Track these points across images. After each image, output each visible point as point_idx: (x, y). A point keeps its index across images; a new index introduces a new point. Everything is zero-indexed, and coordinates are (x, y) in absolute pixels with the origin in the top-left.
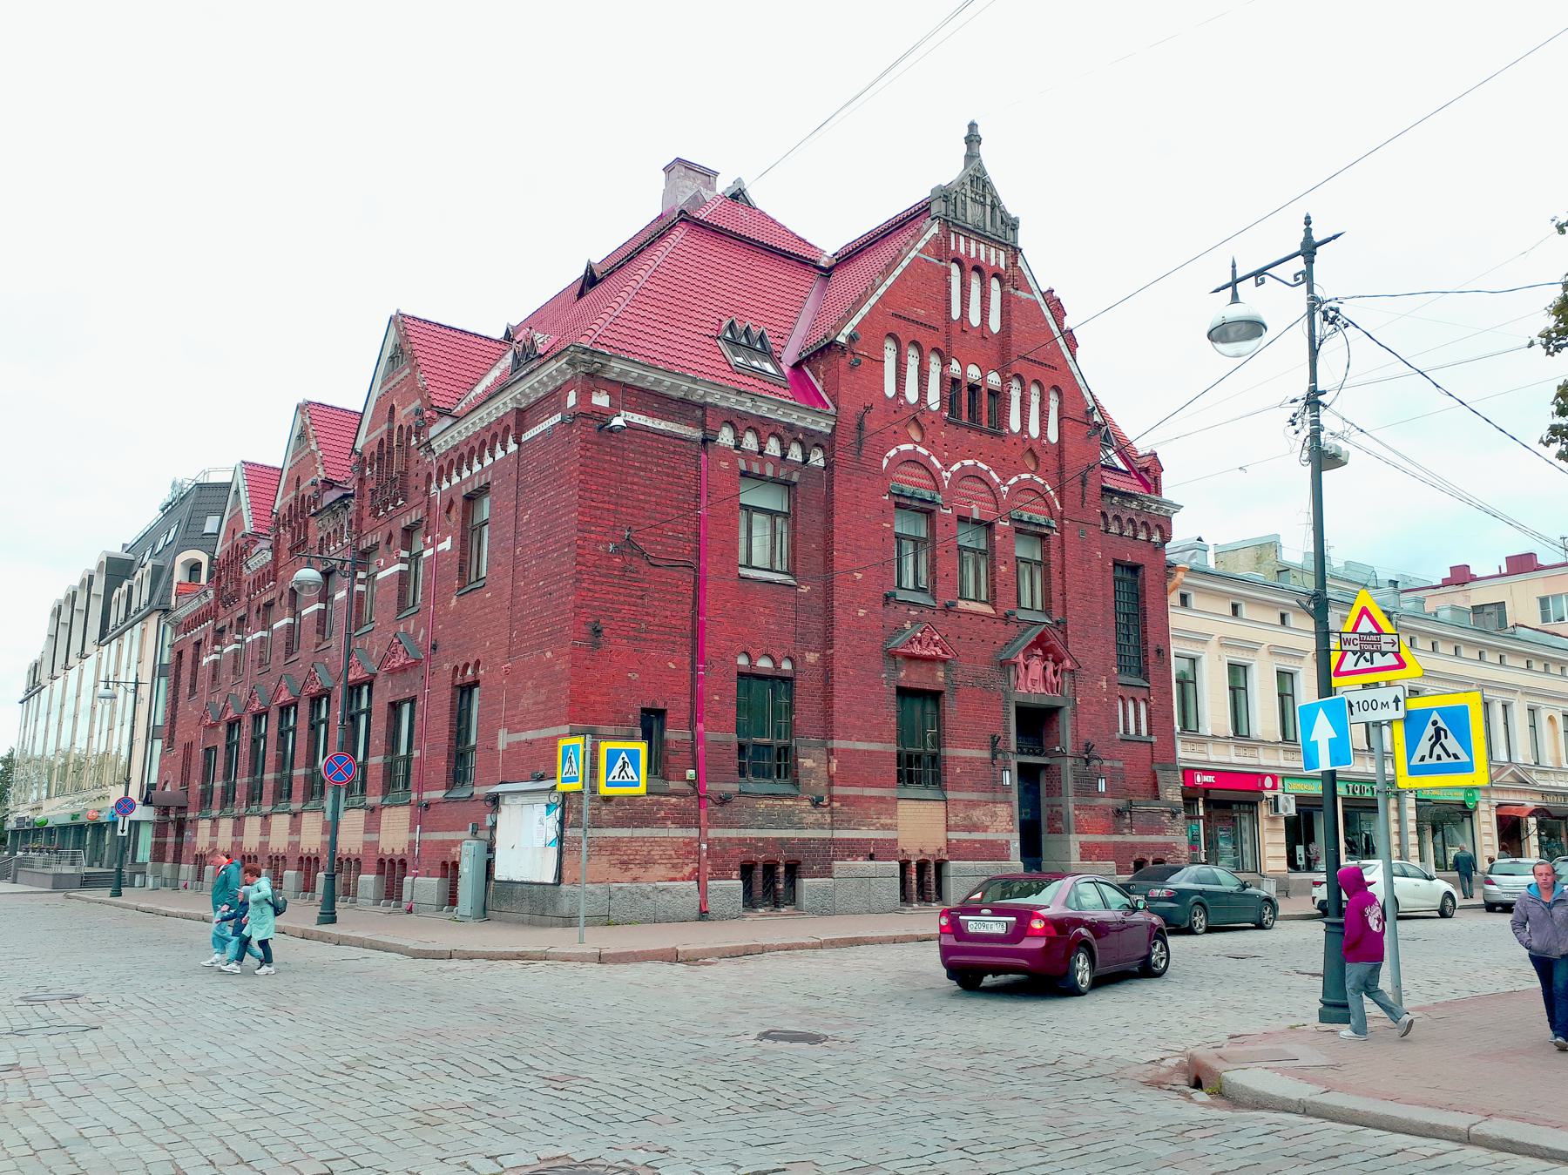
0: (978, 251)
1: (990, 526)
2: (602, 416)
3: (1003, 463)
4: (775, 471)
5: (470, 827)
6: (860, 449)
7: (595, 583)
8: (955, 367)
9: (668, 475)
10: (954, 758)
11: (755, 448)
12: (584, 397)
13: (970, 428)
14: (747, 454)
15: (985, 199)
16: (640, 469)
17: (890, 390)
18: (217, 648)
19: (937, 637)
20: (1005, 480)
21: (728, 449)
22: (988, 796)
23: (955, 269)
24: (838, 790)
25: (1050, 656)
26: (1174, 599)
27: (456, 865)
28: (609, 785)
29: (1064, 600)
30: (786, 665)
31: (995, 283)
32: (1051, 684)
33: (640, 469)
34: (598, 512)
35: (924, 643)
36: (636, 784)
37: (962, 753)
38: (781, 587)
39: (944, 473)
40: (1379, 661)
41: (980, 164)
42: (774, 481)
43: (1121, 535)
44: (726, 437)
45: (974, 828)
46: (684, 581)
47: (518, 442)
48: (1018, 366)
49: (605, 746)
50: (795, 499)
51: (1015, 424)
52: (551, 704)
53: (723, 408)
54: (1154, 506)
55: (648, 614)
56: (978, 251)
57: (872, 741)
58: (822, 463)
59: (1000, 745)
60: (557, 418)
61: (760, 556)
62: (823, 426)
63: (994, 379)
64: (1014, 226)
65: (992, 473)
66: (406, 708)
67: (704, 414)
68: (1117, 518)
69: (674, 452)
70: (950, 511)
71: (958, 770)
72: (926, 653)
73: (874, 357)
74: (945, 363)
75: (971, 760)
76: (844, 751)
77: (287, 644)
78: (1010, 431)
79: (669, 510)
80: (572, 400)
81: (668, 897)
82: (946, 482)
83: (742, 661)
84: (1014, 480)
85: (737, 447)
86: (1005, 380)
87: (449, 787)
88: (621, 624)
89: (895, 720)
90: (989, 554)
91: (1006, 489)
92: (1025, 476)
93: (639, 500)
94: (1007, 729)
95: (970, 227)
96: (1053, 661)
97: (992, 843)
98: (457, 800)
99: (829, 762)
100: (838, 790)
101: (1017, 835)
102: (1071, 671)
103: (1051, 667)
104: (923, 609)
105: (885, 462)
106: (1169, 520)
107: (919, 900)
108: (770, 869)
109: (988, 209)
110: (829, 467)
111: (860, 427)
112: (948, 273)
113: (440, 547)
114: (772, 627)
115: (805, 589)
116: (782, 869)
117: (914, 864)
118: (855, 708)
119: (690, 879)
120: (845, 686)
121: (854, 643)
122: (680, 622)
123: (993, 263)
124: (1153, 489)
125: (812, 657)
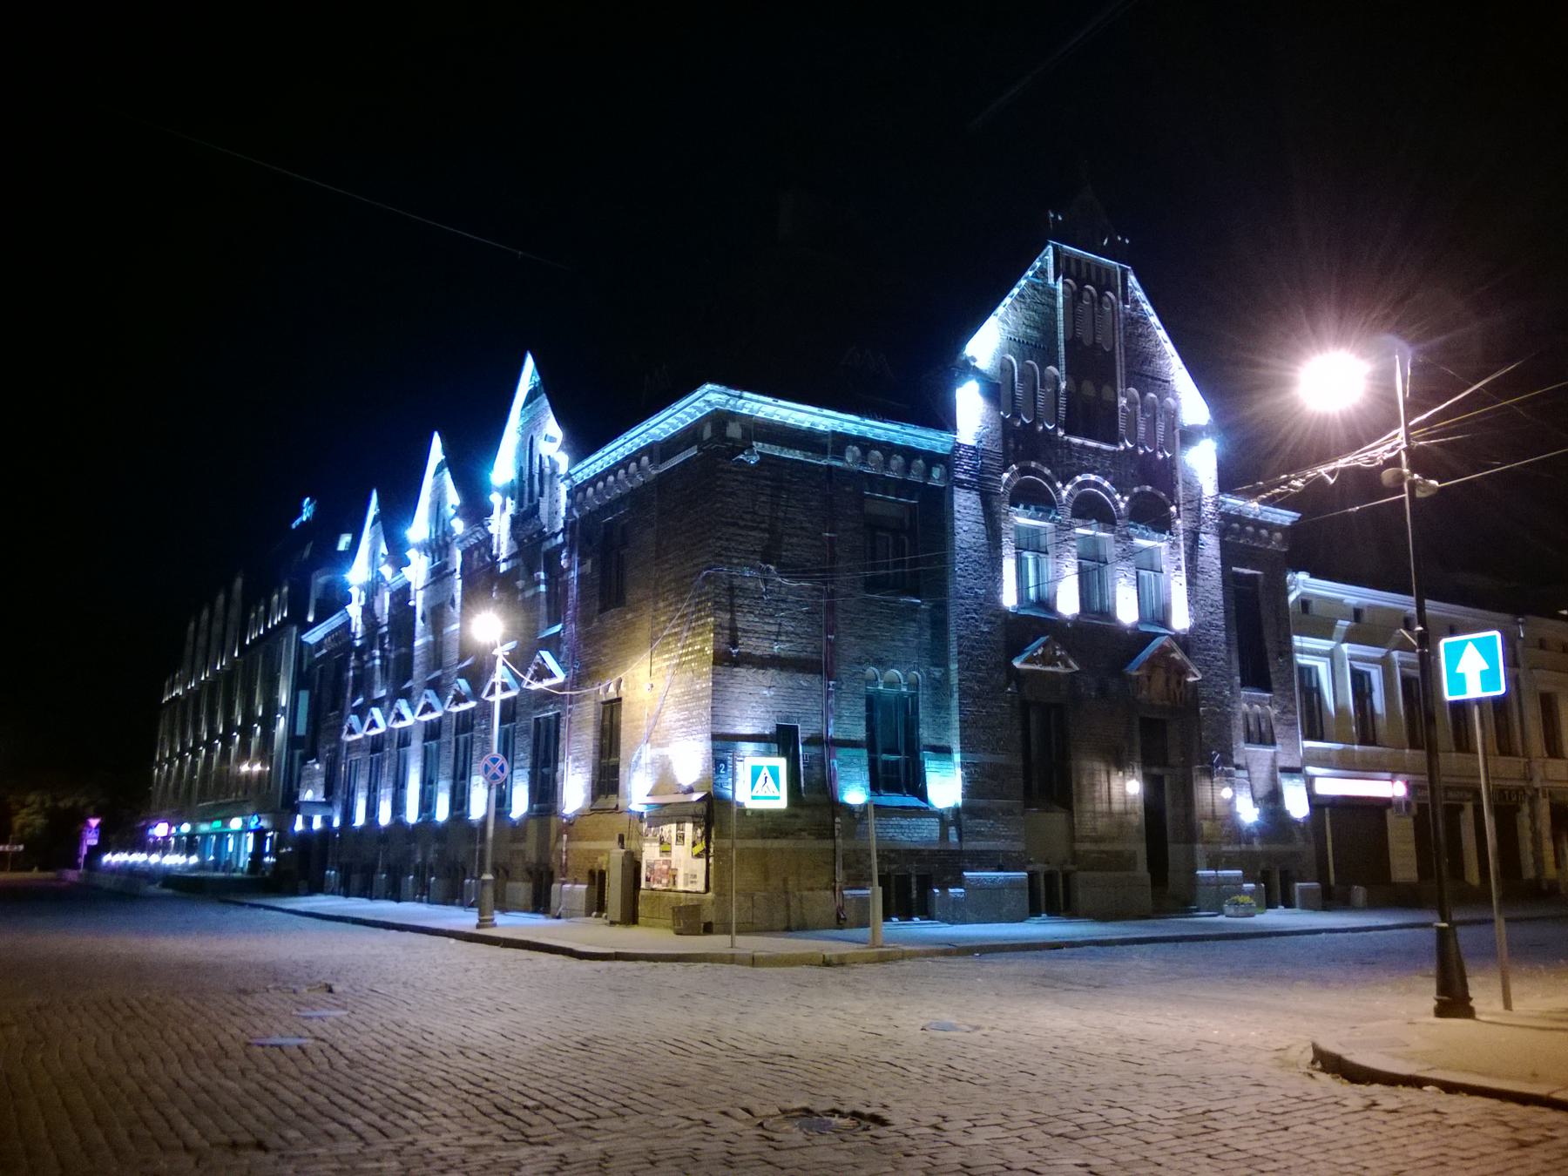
27: (602, 874)
36: (778, 798)
97: (1119, 854)
108: (904, 881)
116: (914, 880)
119: (826, 889)
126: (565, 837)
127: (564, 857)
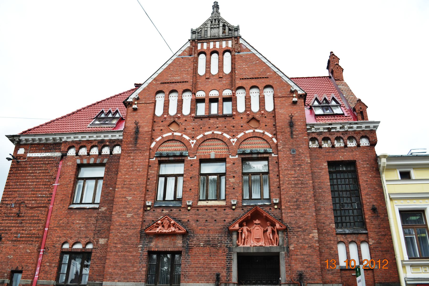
2: (23, 156)
3: (233, 128)
9: (43, 173)
14: (81, 157)
15: (219, 25)
19: (173, 222)
33: (31, 173)
34: (11, 193)
35: (166, 226)
38: (90, 210)
46: (42, 214)
53: (69, 142)
55: (23, 230)
57: (128, 281)
64: (237, 29)
70: (195, 158)
73: (148, 102)
79: (41, 186)
82: (192, 145)
88: (10, 235)
89: (144, 269)
91: (235, 140)
93: (29, 185)
103: (270, 229)
104: (172, 209)
109: (221, 28)
114: (82, 229)
115: (103, 209)
118: (119, 264)
120: (113, 253)
121: (122, 231)
122: (37, 232)
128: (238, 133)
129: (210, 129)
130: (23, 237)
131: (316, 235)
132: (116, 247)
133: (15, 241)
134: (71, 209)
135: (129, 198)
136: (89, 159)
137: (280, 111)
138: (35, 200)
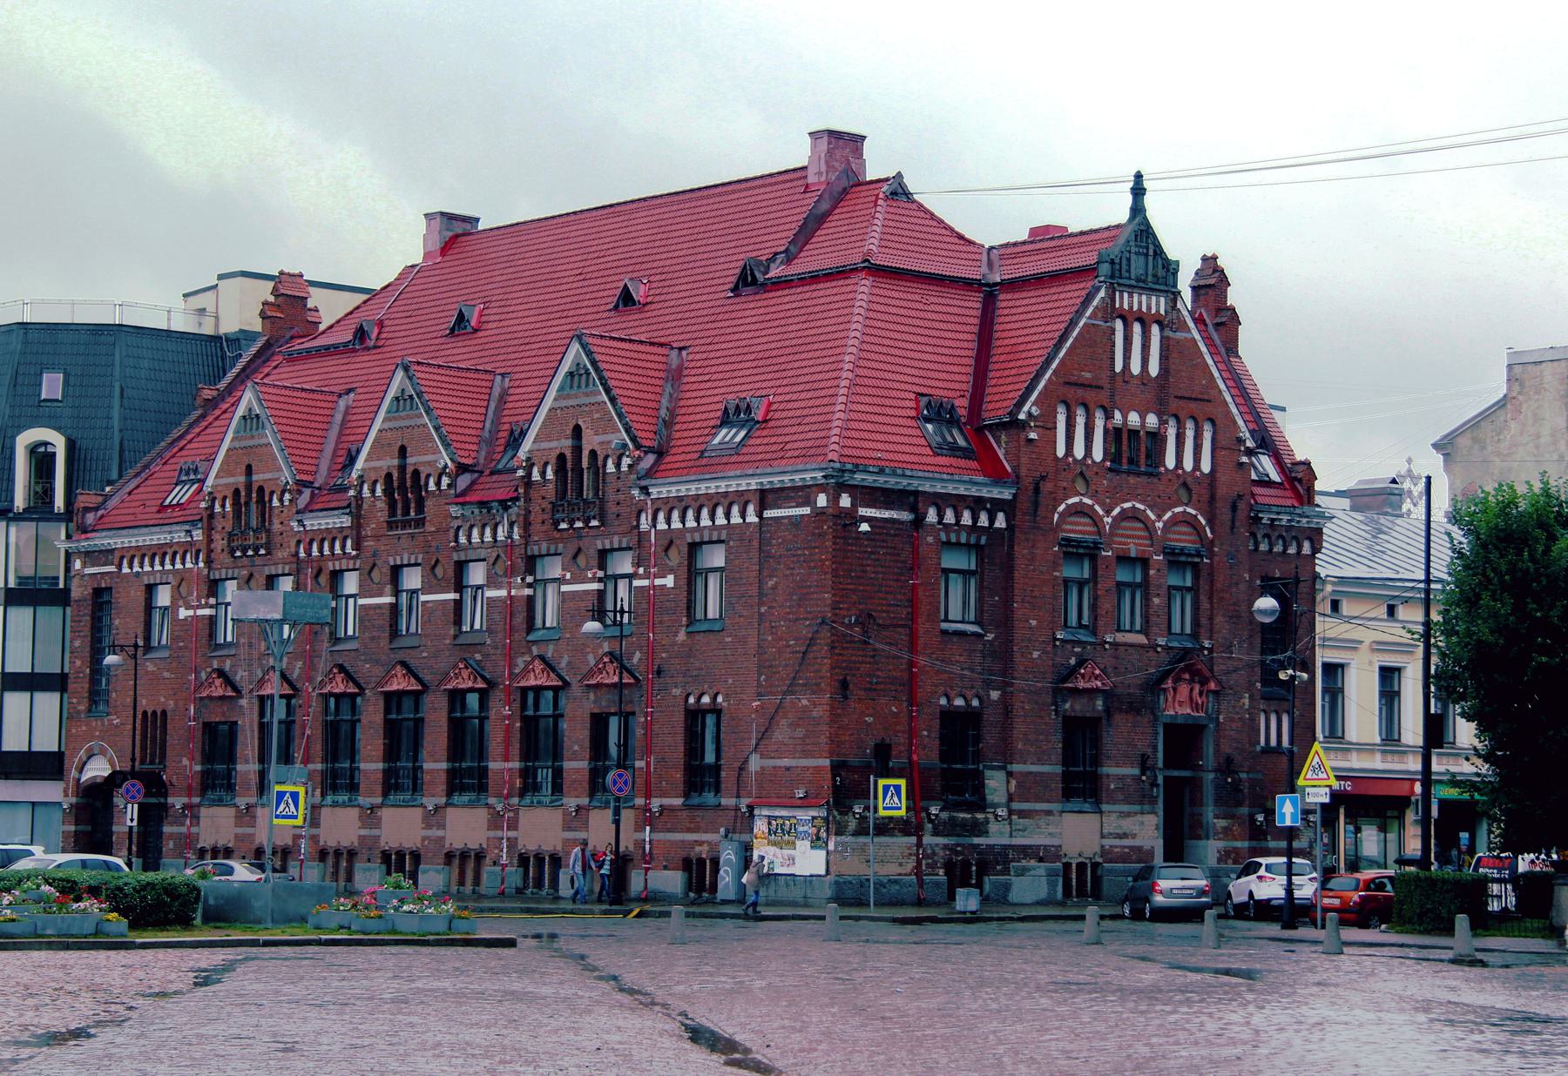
0: (1140, 303)
1: (1144, 562)
4: (968, 539)
5: (722, 830)
6: (1036, 511)
7: (843, 648)
8: (1118, 415)
10: (1108, 776)
11: (953, 521)
12: (834, 499)
13: (1129, 473)
14: (947, 526)
15: (1147, 248)
16: (872, 553)
17: (1061, 451)
18: (212, 601)
19: (1097, 672)
20: (1159, 517)
21: (932, 525)
22: (1137, 808)
23: (1119, 325)
24: (1016, 806)
25: (1196, 678)
26: (1324, 607)
28: (885, 808)
29: (1211, 624)
30: (975, 703)
31: (1155, 329)
32: (1197, 704)
33: (872, 553)
36: (900, 808)
37: (1117, 770)
39: (1106, 519)
40: (1321, 776)
41: (1145, 218)
42: (968, 546)
43: (1270, 551)
44: (932, 516)
45: (1124, 836)
47: (760, 516)
48: (1174, 405)
49: (882, 782)
50: (982, 559)
51: (1170, 462)
52: (807, 741)
53: (929, 493)
54: (1305, 520)
55: (878, 670)
56: (1140, 303)
58: (1004, 525)
59: (1149, 763)
60: (806, 510)
61: (955, 611)
62: (1007, 494)
63: (1152, 420)
65: (1149, 512)
66: (614, 723)
67: (916, 502)
68: (1266, 536)
69: (895, 535)
71: (1112, 786)
72: (1088, 685)
74: (1109, 416)
75: (1121, 778)
76: (1020, 773)
77: (391, 626)
78: (1166, 469)
80: (822, 500)
81: (897, 887)
83: (943, 701)
84: (1169, 514)
85: (940, 522)
86: (1163, 422)
87: (687, 795)
90: (1145, 585)
92: (1178, 509)
94: (1155, 748)
95: (1133, 283)
96: (1199, 682)
98: (699, 807)
99: (1008, 782)
100: (1016, 806)
101: (1161, 842)
102: (1216, 693)
103: (1197, 688)
105: (1056, 516)
106: (1319, 531)
107: (1077, 896)
109: (1151, 259)
110: (1010, 527)
111: (1037, 490)
112: (1113, 331)
113: (658, 582)
114: (965, 672)
116: (974, 868)
117: (1074, 866)
123: (1153, 311)
124: (1306, 500)
125: (995, 695)
126: (648, 828)
127: (647, 847)
128: (1164, 512)
129: (1134, 497)
130: (881, 683)
131: (1247, 701)
132: (1023, 708)
133: (870, 689)
134: (945, 632)
135: (1034, 623)
136: (958, 534)
137: (1222, 478)
138: (888, 612)
